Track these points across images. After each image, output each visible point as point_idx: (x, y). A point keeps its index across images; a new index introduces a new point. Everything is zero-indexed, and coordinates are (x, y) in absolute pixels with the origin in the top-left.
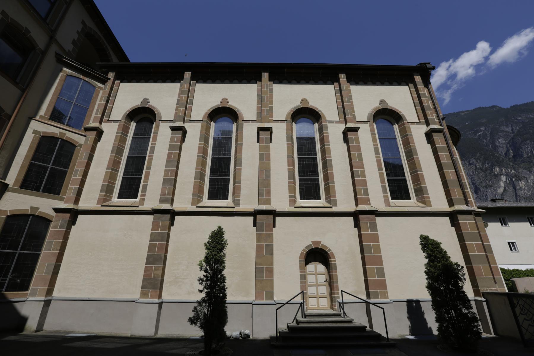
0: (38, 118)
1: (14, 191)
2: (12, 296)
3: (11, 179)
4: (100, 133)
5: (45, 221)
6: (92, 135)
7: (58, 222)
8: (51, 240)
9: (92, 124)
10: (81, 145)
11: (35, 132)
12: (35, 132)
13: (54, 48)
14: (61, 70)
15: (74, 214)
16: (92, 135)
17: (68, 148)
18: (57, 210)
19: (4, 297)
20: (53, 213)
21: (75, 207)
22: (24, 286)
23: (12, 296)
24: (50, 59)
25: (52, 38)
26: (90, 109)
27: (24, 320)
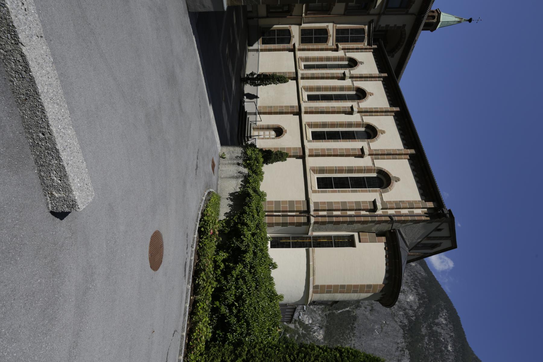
0: (335, 25)
1: (299, 28)
2: (260, 40)
3: (304, 26)
4: (336, 50)
5: (289, 41)
6: (335, 47)
7: (290, 46)
8: (281, 46)
9: (340, 46)
10: (327, 45)
11: (328, 26)
12: (328, 26)
13: (375, 18)
14: (365, 25)
15: (293, 50)
16: (335, 47)
17: (325, 40)
18: (294, 45)
19: (260, 38)
20: (293, 43)
21: (296, 49)
22: (263, 43)
23: (260, 40)
24: (369, 18)
25: (379, 15)
26: (349, 43)
27: (252, 45)
